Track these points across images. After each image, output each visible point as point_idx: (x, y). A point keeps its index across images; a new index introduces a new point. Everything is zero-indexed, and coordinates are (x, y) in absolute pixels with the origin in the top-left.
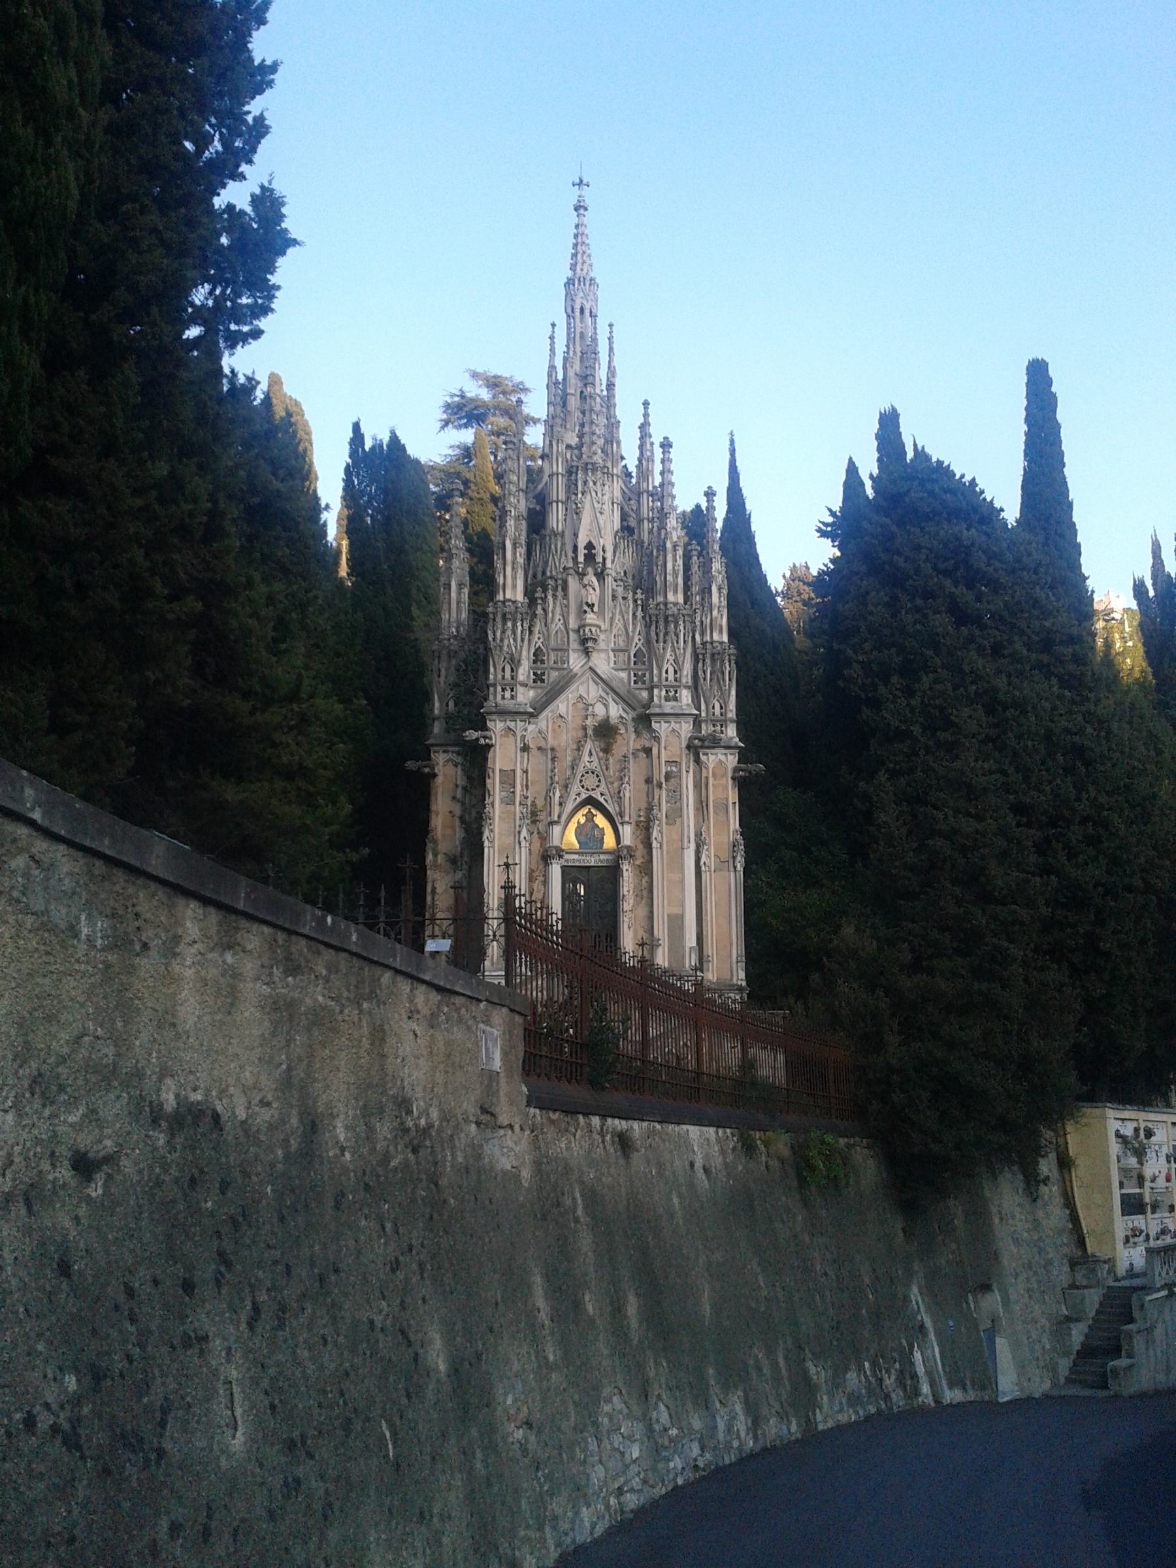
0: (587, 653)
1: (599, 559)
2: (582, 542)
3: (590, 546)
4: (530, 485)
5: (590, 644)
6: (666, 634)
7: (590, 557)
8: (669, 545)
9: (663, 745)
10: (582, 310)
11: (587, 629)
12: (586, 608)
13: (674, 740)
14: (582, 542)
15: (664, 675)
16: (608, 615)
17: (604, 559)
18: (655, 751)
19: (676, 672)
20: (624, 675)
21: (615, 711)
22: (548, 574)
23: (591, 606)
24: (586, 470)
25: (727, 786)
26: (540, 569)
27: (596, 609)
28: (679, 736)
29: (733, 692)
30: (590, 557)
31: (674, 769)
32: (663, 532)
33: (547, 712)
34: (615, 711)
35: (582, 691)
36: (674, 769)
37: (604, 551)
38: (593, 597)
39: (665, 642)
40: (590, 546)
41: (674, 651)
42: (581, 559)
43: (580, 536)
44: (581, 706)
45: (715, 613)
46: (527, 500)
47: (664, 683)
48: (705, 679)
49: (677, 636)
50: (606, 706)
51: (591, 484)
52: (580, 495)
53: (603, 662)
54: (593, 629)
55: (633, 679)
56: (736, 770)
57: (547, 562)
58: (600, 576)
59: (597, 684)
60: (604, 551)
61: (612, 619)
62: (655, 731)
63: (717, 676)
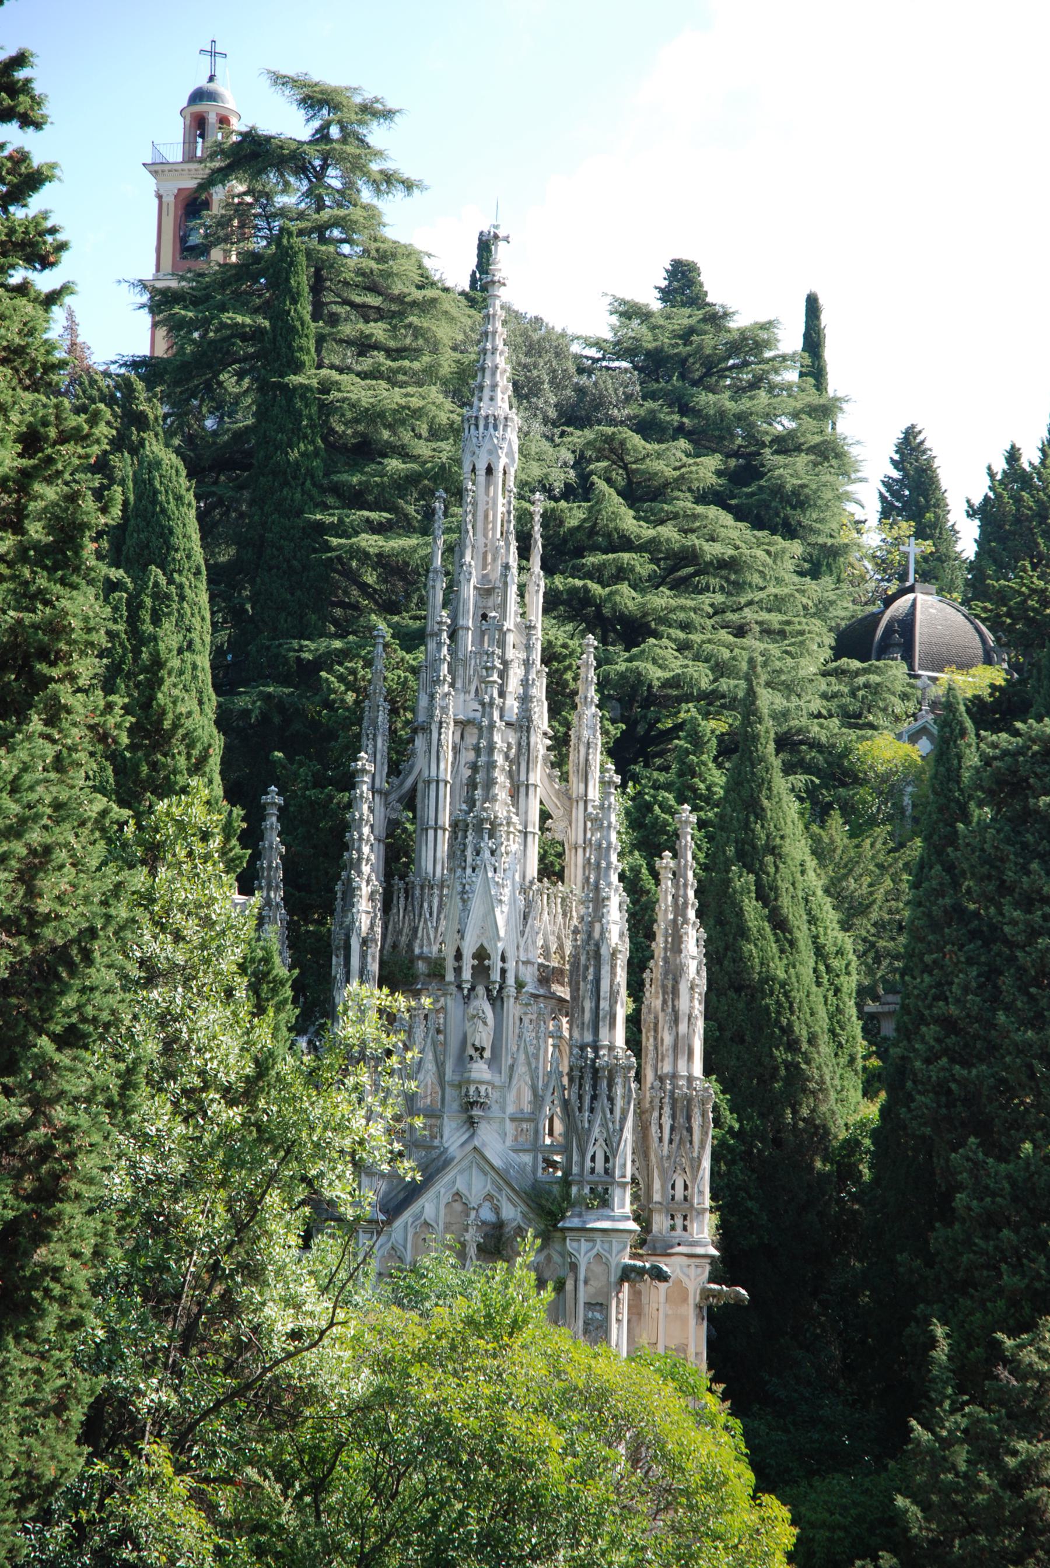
0: (471, 1123)
1: (496, 976)
2: (469, 950)
3: (481, 954)
4: (393, 779)
5: (476, 1112)
6: (594, 1098)
7: (481, 970)
8: (604, 951)
9: (582, 1276)
10: (489, 471)
11: (472, 1089)
12: (471, 1051)
13: (598, 1269)
14: (469, 950)
15: (588, 1164)
16: (506, 1062)
17: (503, 971)
18: (569, 1286)
19: (607, 1159)
20: (527, 1158)
21: (511, 1212)
22: (417, 951)
23: (481, 1050)
24: (479, 830)
25: (684, 1320)
26: (404, 939)
27: (487, 1054)
28: (607, 1265)
29: (706, 1164)
30: (481, 970)
31: (598, 1315)
32: (597, 926)
33: (407, 1216)
34: (511, 1212)
35: (460, 1185)
36: (598, 1315)
37: (503, 959)
38: (484, 1036)
39: (592, 1110)
40: (481, 954)
41: (604, 1125)
42: (467, 974)
43: (468, 937)
44: (458, 1207)
45: (683, 1028)
46: (387, 805)
47: (591, 1178)
48: (661, 1139)
49: (611, 1099)
50: (497, 1210)
51: (487, 854)
52: (469, 871)
53: (496, 1142)
54: (482, 1089)
55: (541, 1165)
56: (706, 1294)
57: (415, 930)
58: (497, 1000)
59: (486, 1174)
60: (503, 959)
61: (512, 1067)
62: (570, 1255)
63: (682, 1130)
